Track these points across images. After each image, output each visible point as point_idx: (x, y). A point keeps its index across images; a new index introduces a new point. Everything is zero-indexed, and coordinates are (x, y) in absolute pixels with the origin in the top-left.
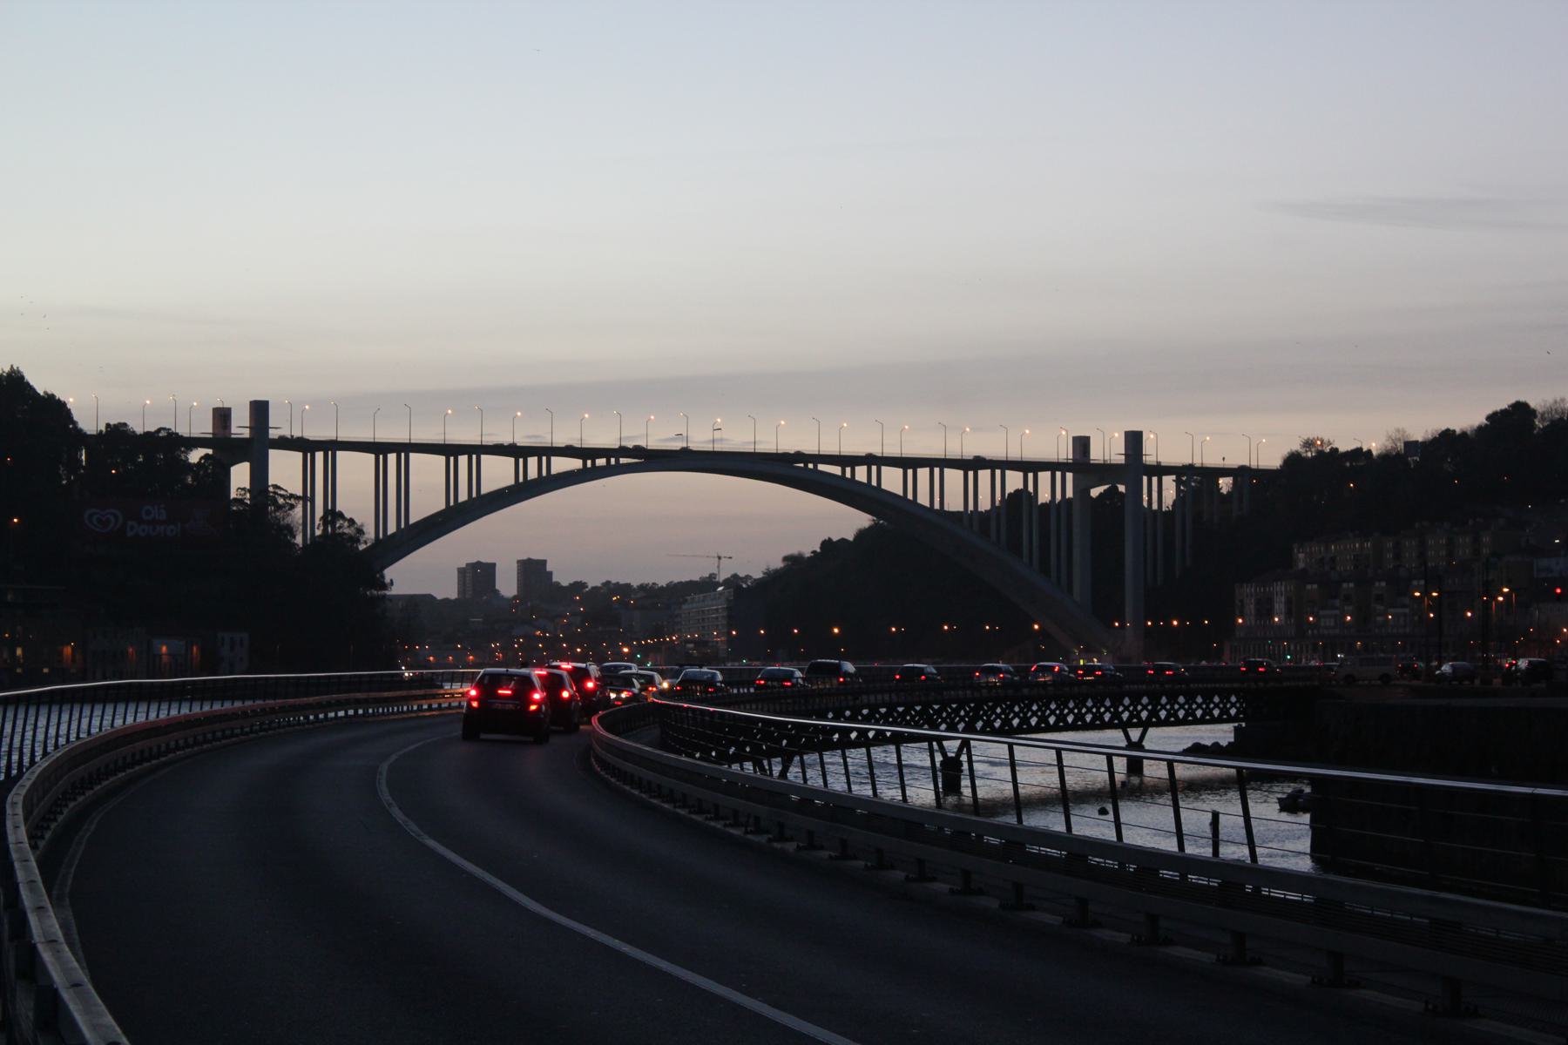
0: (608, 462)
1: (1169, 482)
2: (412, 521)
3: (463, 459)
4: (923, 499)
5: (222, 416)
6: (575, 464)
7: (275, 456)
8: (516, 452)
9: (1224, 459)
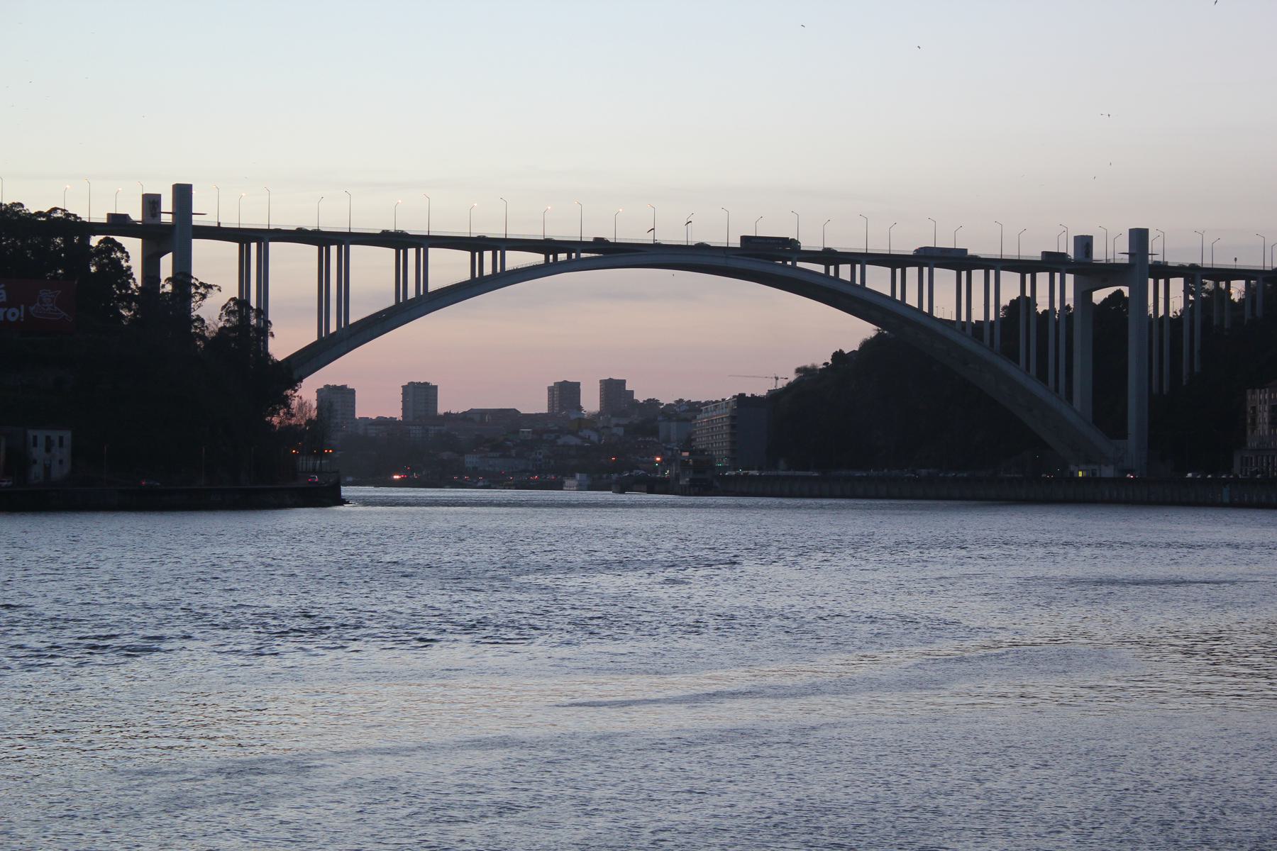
0: (569, 256)
1: (1177, 284)
2: (351, 321)
3: (412, 252)
4: (912, 300)
5: (152, 203)
6: (537, 258)
7: (200, 247)
8: (475, 245)
9: (1236, 259)
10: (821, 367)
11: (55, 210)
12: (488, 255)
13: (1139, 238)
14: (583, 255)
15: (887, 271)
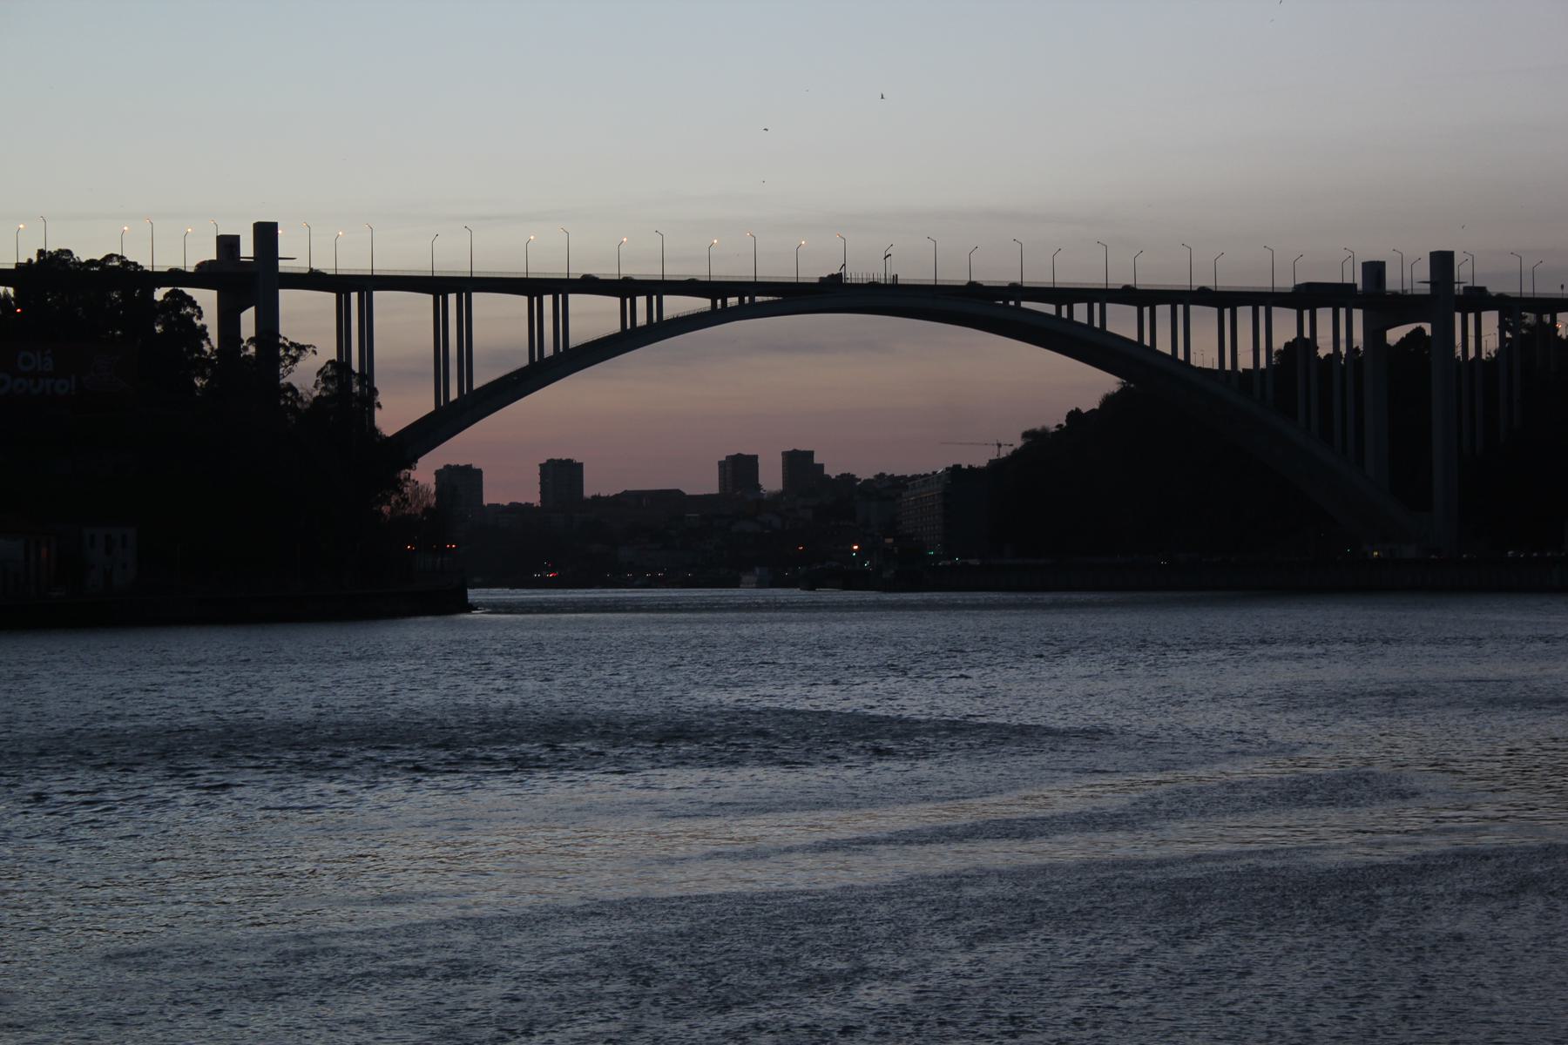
0: (741, 300)
1: (1491, 319)
2: (476, 386)
4: (1164, 345)
5: (228, 244)
6: (702, 304)
7: (290, 300)
8: (624, 288)
9: (1562, 287)
10: (1054, 430)
11: (110, 257)
12: (641, 301)
13: (1442, 262)
14: (758, 299)
15: (1132, 310)
